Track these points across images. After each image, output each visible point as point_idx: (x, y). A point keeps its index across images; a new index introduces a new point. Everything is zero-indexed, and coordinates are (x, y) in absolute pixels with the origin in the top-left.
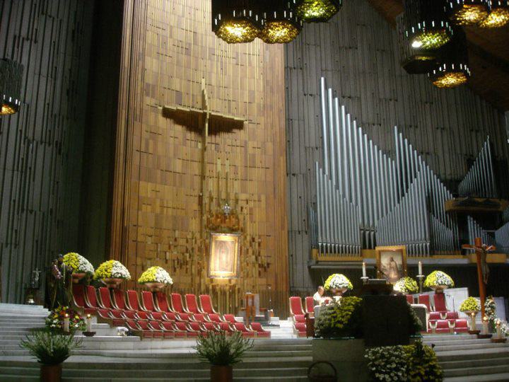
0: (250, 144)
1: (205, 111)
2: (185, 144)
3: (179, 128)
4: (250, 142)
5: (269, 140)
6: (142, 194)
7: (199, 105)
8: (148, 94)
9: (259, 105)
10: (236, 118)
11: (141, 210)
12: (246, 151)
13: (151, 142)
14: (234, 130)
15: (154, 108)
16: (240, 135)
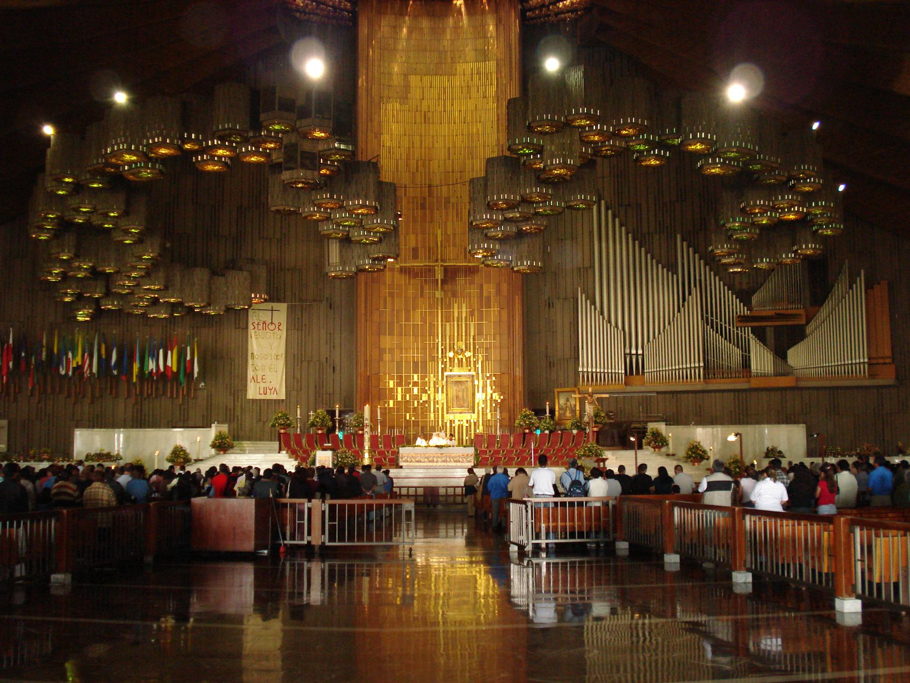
5: (503, 281)
6: (382, 346)
11: (382, 360)
16: (477, 279)
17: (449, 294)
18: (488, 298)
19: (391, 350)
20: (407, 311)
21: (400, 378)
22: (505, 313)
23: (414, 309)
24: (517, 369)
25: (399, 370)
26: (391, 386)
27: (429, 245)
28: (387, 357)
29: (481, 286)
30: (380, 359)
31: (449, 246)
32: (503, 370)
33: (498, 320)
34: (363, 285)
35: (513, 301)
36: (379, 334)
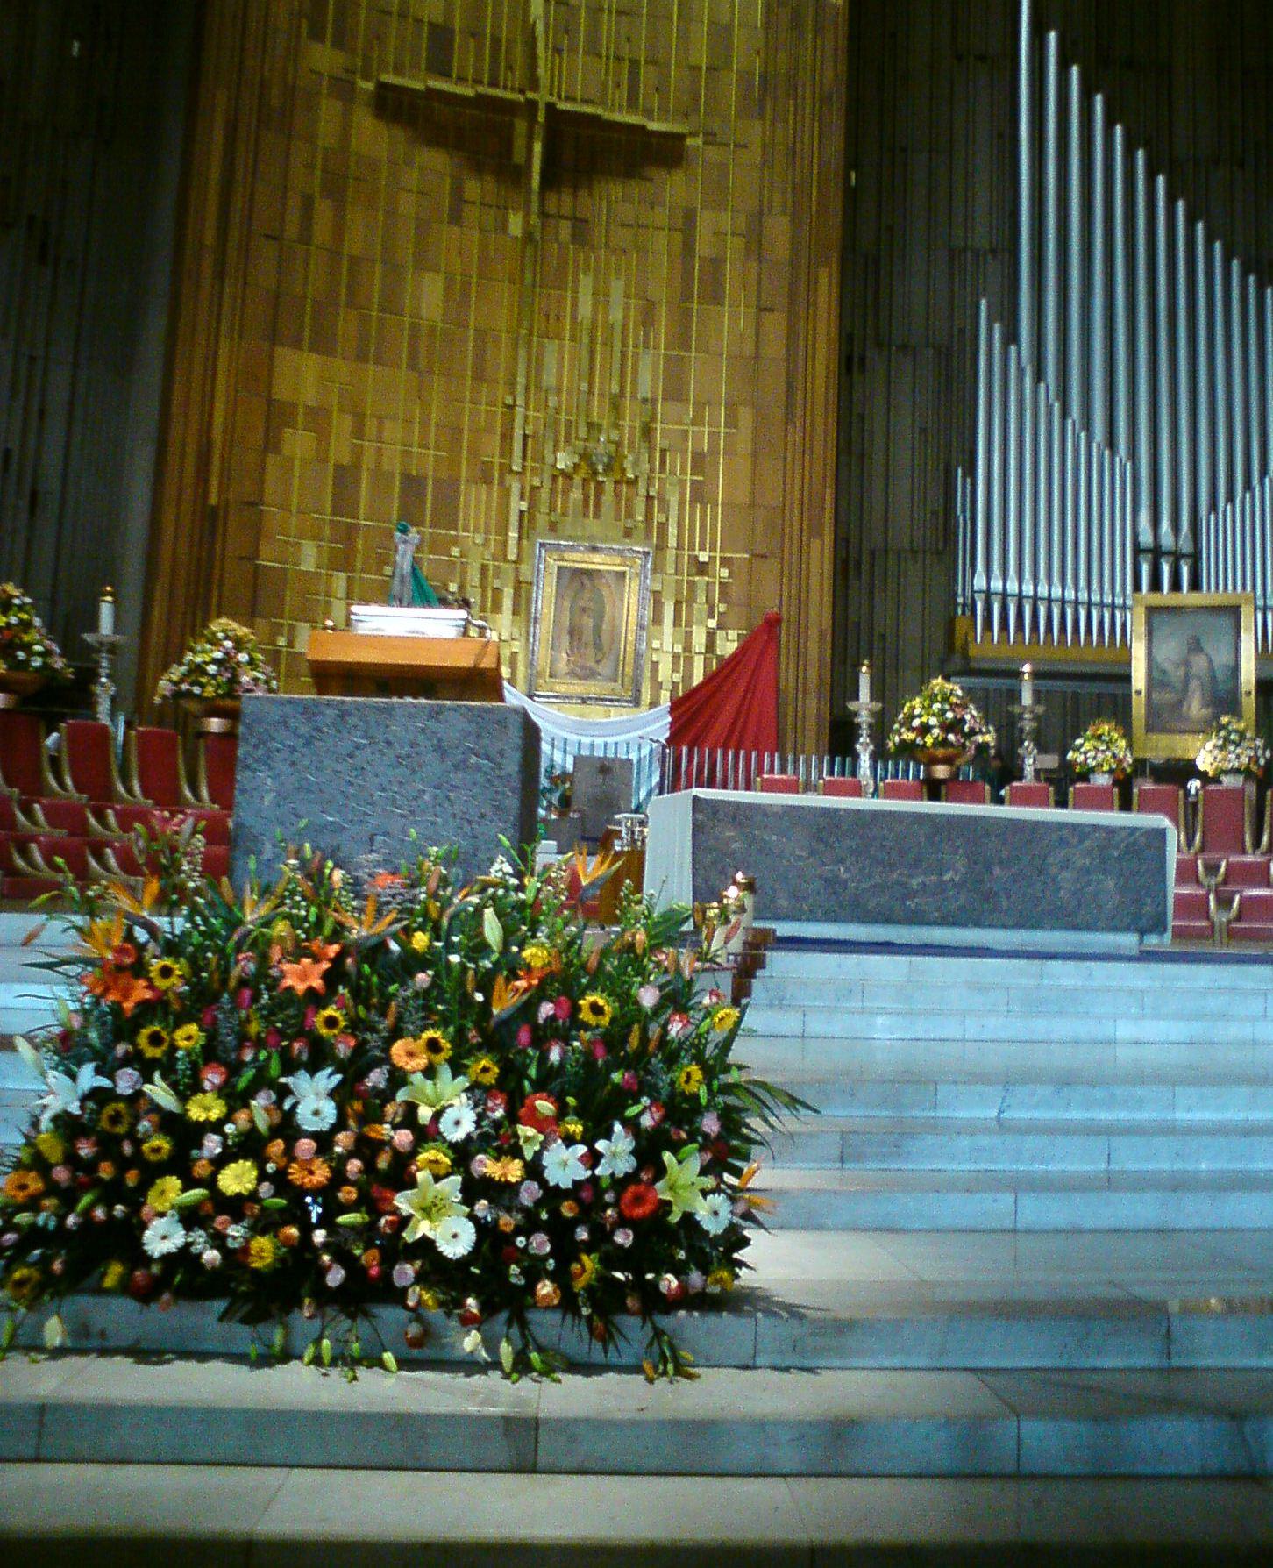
0: (705, 222)
1: (530, 95)
2: (456, 217)
3: (436, 161)
4: (706, 214)
5: (777, 205)
6: (282, 391)
7: (518, 77)
8: (317, 35)
9: (745, 78)
10: (653, 126)
12: (688, 246)
13: (324, 210)
14: (655, 173)
15: (343, 89)
16: (674, 186)
17: (565, 229)
18: (717, 263)
19: (318, 419)
20: (394, 271)
21: (348, 535)
22: (775, 324)
23: (422, 262)
24: (816, 544)
25: (344, 502)
26: (308, 565)
27: (497, 27)
28: (298, 442)
29: (690, 218)
30: (271, 444)
31: (573, 49)
32: (762, 549)
33: (749, 349)
34: (218, 136)
35: (813, 282)
36: (274, 338)
